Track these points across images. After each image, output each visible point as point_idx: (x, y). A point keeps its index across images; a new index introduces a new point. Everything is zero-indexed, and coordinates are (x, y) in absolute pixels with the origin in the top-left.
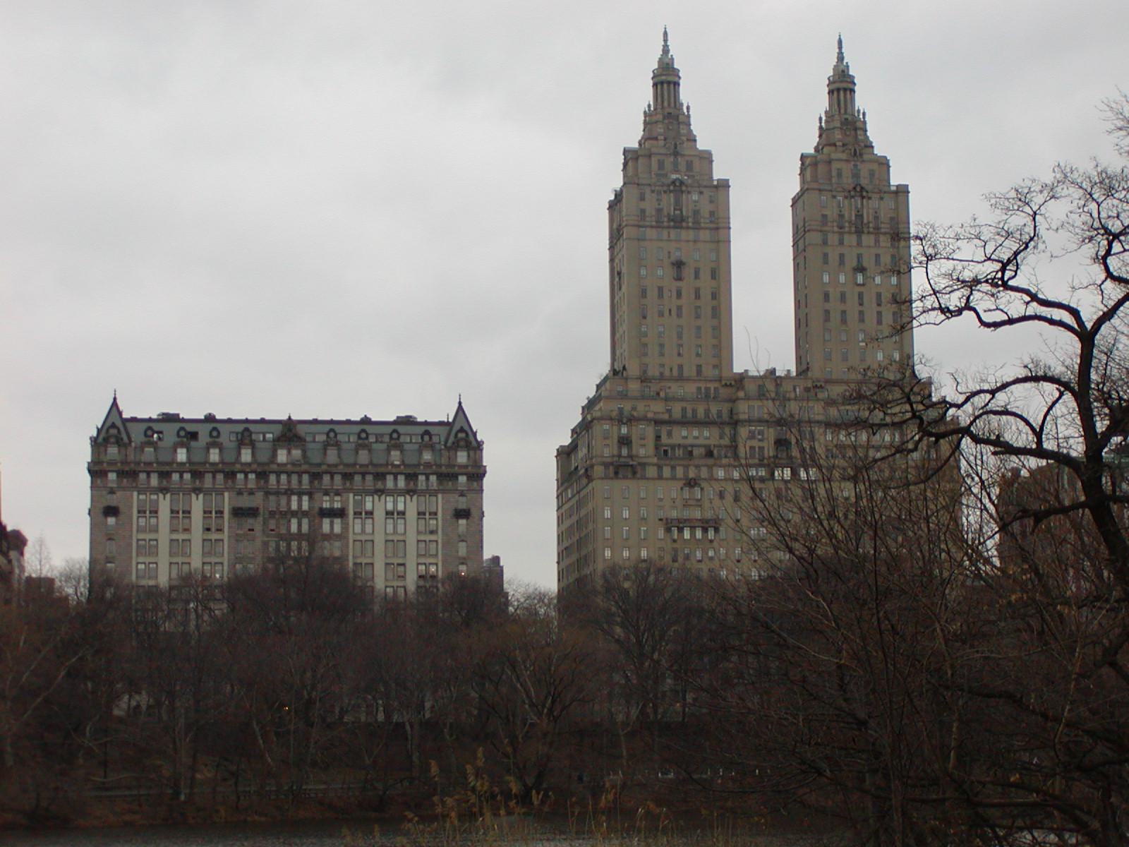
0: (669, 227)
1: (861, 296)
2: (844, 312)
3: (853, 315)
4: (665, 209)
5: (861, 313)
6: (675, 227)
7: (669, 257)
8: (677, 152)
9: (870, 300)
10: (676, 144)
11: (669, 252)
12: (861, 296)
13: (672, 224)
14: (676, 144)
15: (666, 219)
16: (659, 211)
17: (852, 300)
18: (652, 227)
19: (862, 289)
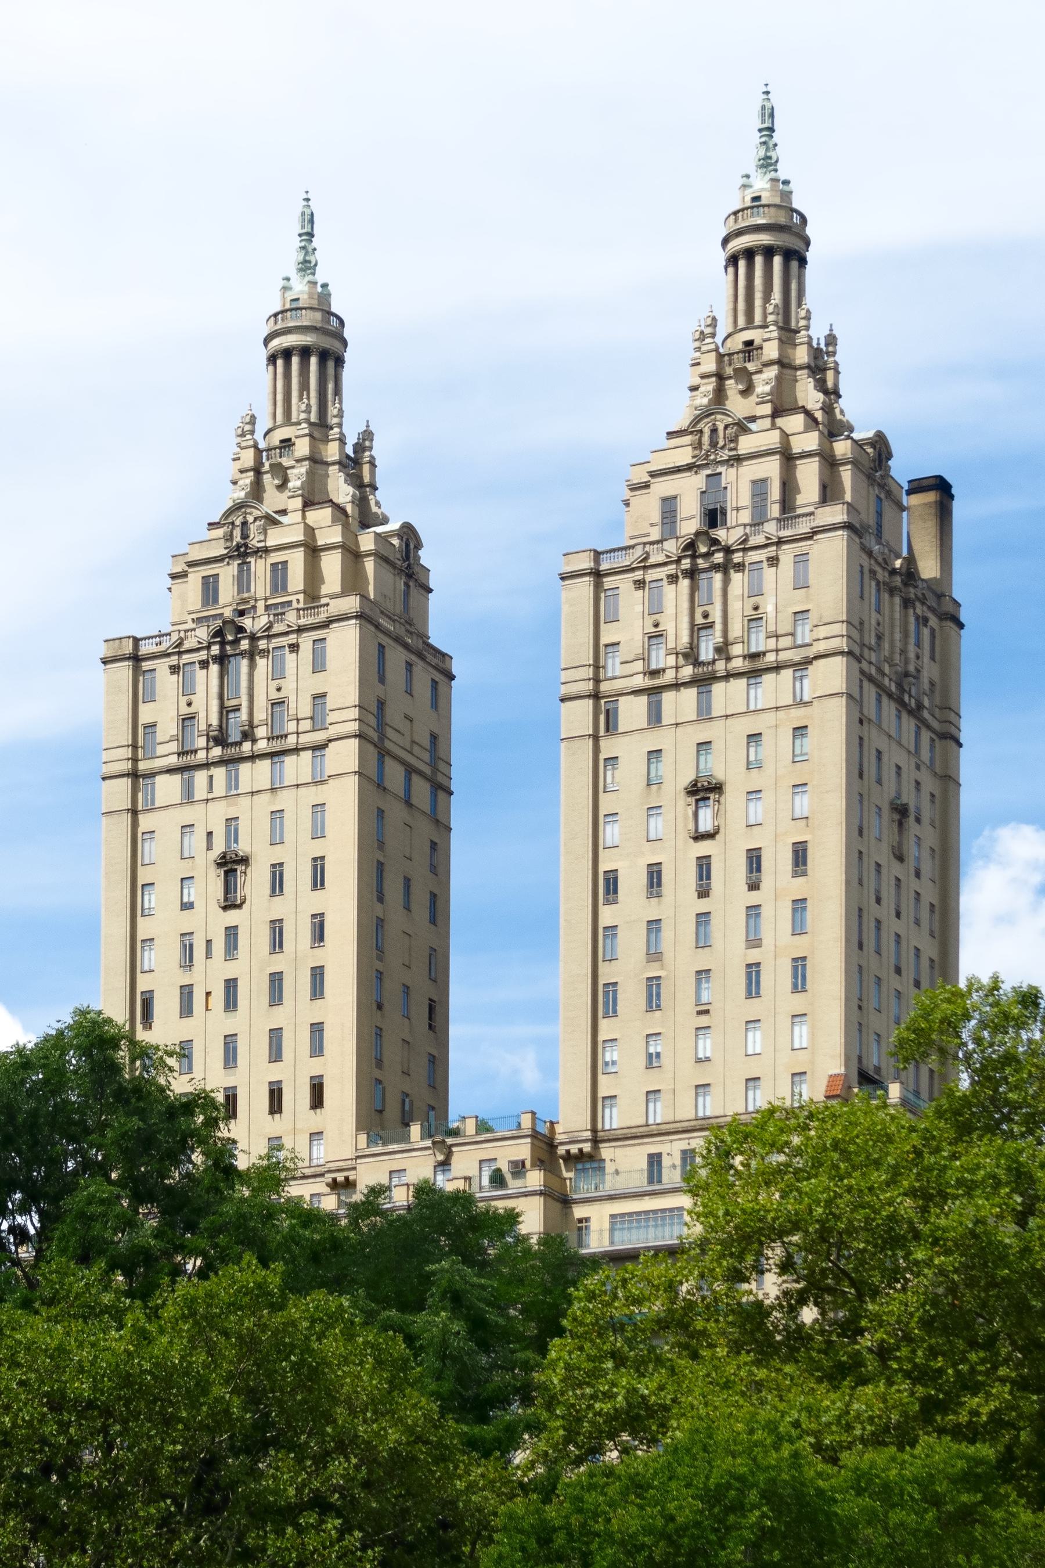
0: (206, 765)
1: (704, 866)
2: (654, 926)
3: (678, 935)
4: (202, 715)
5: (703, 918)
6: (222, 762)
7: (209, 848)
8: (246, 545)
9: (730, 872)
10: (245, 524)
11: (210, 834)
12: (704, 866)
13: (217, 752)
14: (245, 524)
15: (202, 742)
16: (187, 720)
17: (680, 879)
18: (170, 771)
19: (704, 848)
